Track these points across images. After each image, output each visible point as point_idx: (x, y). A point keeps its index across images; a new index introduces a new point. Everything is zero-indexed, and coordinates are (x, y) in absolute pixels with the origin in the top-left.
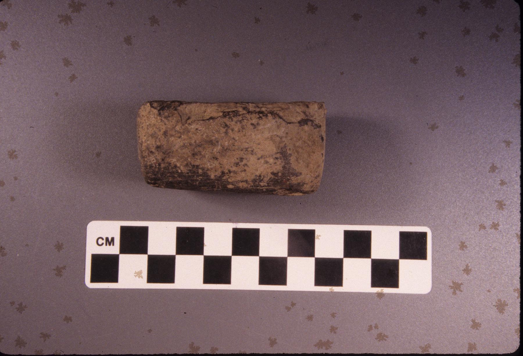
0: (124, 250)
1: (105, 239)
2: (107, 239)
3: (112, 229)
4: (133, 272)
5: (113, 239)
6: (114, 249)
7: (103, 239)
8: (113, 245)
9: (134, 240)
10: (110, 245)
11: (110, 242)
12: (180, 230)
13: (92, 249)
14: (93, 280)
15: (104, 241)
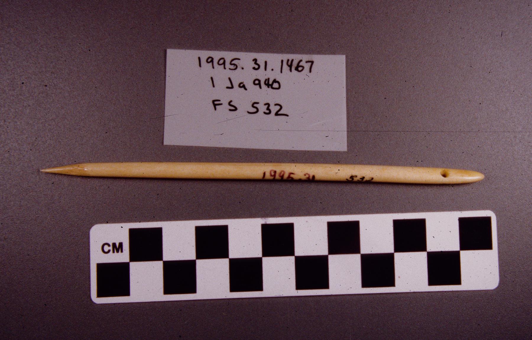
0: (135, 256)
1: (111, 244)
2: (114, 245)
3: (119, 232)
4: (147, 283)
5: (121, 244)
6: (124, 257)
7: (109, 245)
8: (122, 251)
9: (146, 245)
10: (118, 252)
11: (118, 248)
12: (199, 230)
13: (97, 257)
14: (99, 295)
15: (111, 248)
